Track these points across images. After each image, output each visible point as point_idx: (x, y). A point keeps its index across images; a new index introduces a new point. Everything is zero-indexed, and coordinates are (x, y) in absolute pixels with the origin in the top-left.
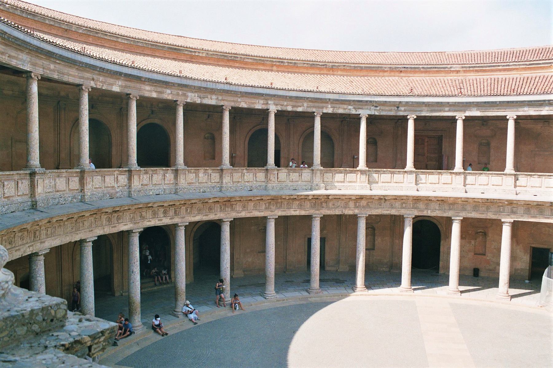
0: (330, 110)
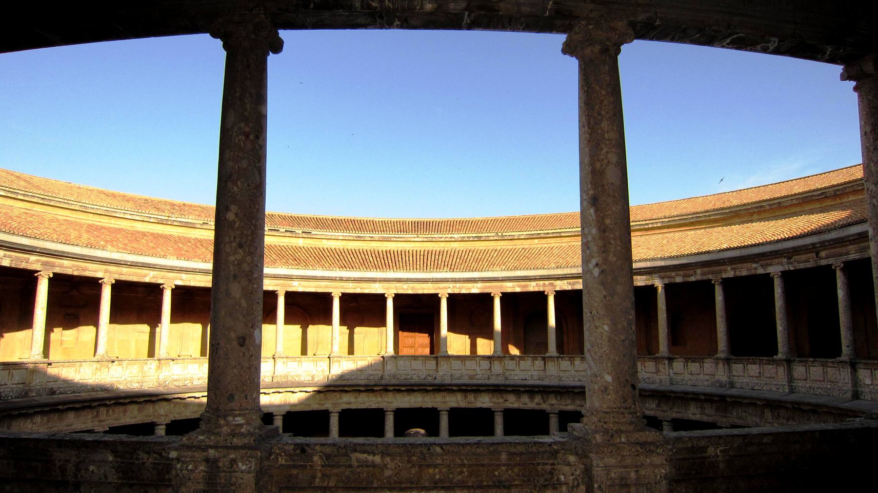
0: (730, 274)
